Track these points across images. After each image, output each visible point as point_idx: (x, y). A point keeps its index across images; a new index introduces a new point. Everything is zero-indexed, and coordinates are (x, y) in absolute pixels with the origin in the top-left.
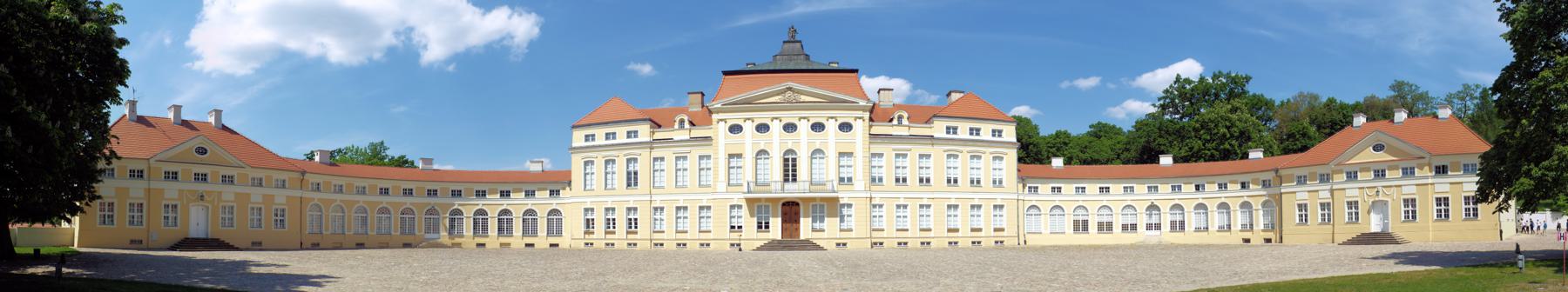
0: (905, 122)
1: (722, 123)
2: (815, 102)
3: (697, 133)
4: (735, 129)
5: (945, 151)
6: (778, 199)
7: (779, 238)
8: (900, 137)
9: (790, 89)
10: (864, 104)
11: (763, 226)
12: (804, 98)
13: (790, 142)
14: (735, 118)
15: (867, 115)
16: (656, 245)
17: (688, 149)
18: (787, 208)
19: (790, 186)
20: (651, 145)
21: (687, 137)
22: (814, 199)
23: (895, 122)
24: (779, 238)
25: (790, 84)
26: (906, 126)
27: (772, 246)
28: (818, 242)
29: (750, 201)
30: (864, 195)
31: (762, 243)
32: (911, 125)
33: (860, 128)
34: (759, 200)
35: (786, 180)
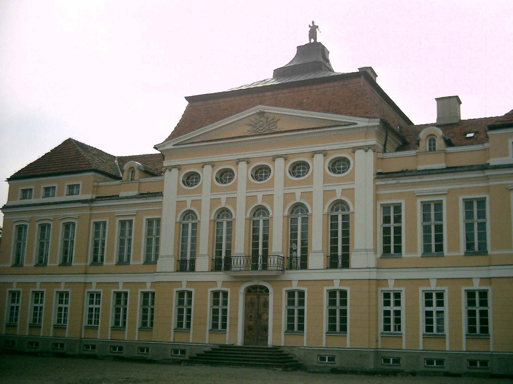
10: (366, 124)
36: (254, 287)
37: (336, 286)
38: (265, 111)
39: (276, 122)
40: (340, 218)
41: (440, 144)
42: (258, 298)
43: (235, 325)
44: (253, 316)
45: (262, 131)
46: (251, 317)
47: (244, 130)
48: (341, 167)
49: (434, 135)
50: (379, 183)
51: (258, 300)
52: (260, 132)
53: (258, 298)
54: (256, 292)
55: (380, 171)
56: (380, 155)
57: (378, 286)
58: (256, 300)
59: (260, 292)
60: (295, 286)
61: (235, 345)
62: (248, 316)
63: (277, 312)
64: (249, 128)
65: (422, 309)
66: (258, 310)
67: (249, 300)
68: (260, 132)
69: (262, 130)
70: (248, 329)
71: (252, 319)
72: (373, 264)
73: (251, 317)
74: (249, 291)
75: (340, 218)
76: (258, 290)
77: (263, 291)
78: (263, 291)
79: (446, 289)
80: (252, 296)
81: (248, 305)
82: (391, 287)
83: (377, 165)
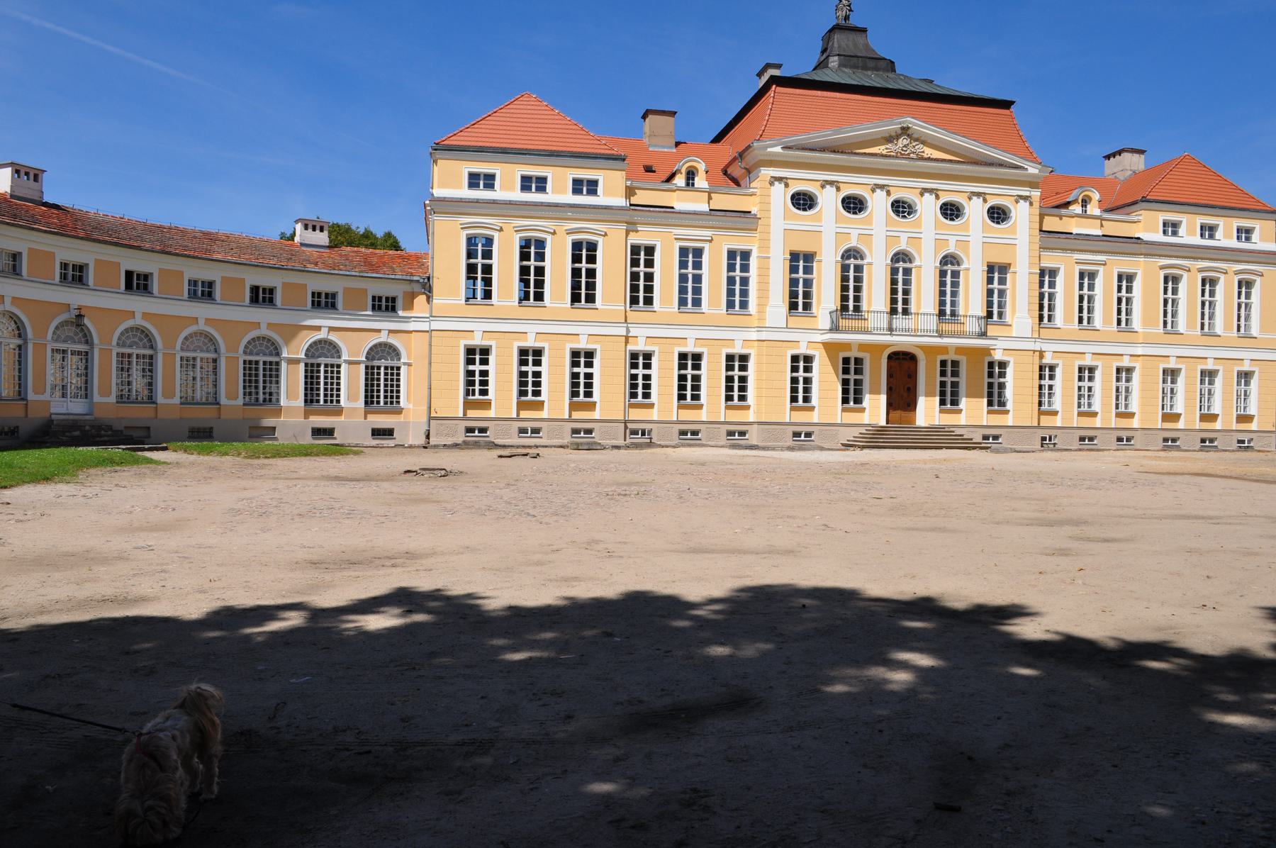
0: (1093, 209)
1: (779, 187)
2: (951, 161)
3: (725, 201)
4: (803, 201)
5: (1162, 268)
6: (884, 346)
7: (882, 422)
8: (1087, 237)
11: (852, 394)
12: (929, 152)
13: (904, 237)
14: (804, 180)
15: (1036, 194)
16: (634, 432)
17: (707, 233)
19: (899, 321)
20: (633, 214)
21: (704, 207)
22: (944, 349)
24: (883, 423)
25: (909, 121)
27: (875, 439)
29: (829, 347)
30: (1031, 346)
32: (1106, 215)
33: (1023, 215)
34: (847, 346)
35: (893, 311)
54: (899, 358)
74: (890, 357)
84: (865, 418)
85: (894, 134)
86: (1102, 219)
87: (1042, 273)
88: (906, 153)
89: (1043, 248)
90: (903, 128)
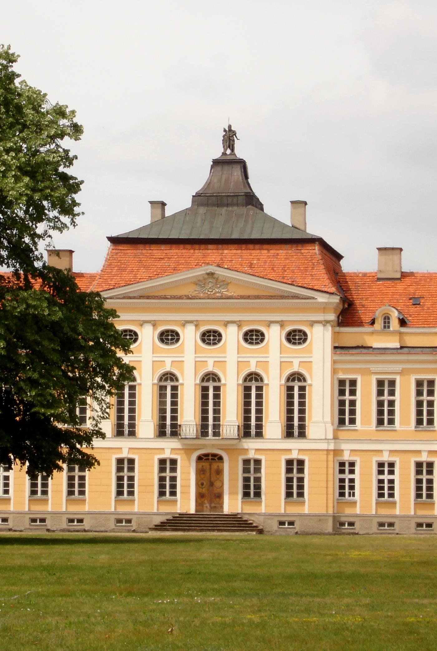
2: (248, 297)
7: (192, 511)
8: (384, 351)
9: (211, 274)
13: (210, 362)
15: (332, 317)
18: (206, 465)
23: (379, 325)
24: (192, 511)
26: (394, 332)
28: (251, 519)
31: (163, 519)
32: (403, 330)
36: (206, 455)
37: (294, 455)
38: (216, 272)
39: (228, 284)
40: (296, 389)
41: (394, 324)
42: (210, 465)
43: (186, 493)
44: (205, 484)
45: (212, 293)
46: (202, 484)
47: (191, 290)
48: (297, 337)
49: (390, 314)
50: (337, 358)
51: (210, 469)
52: (209, 293)
53: (210, 465)
54: (208, 459)
55: (337, 345)
56: (337, 329)
57: (335, 455)
58: (208, 467)
59: (212, 459)
60: (252, 455)
61: (188, 513)
62: (200, 483)
63: (233, 480)
64: (197, 288)
65: (375, 477)
66: (210, 478)
67: (200, 466)
68: (209, 293)
69: (212, 291)
70: (200, 496)
71: (204, 486)
72: (330, 436)
73: (202, 484)
74: (200, 458)
75: (296, 389)
76: (210, 457)
77: (216, 458)
78: (216, 458)
79: (396, 459)
80: (204, 464)
81: (200, 472)
82: (346, 457)
83: (334, 339)
84: (179, 509)
85: (201, 278)
86: (401, 333)
87: (342, 383)
88: (212, 293)
89: (334, 362)
90: (208, 274)
